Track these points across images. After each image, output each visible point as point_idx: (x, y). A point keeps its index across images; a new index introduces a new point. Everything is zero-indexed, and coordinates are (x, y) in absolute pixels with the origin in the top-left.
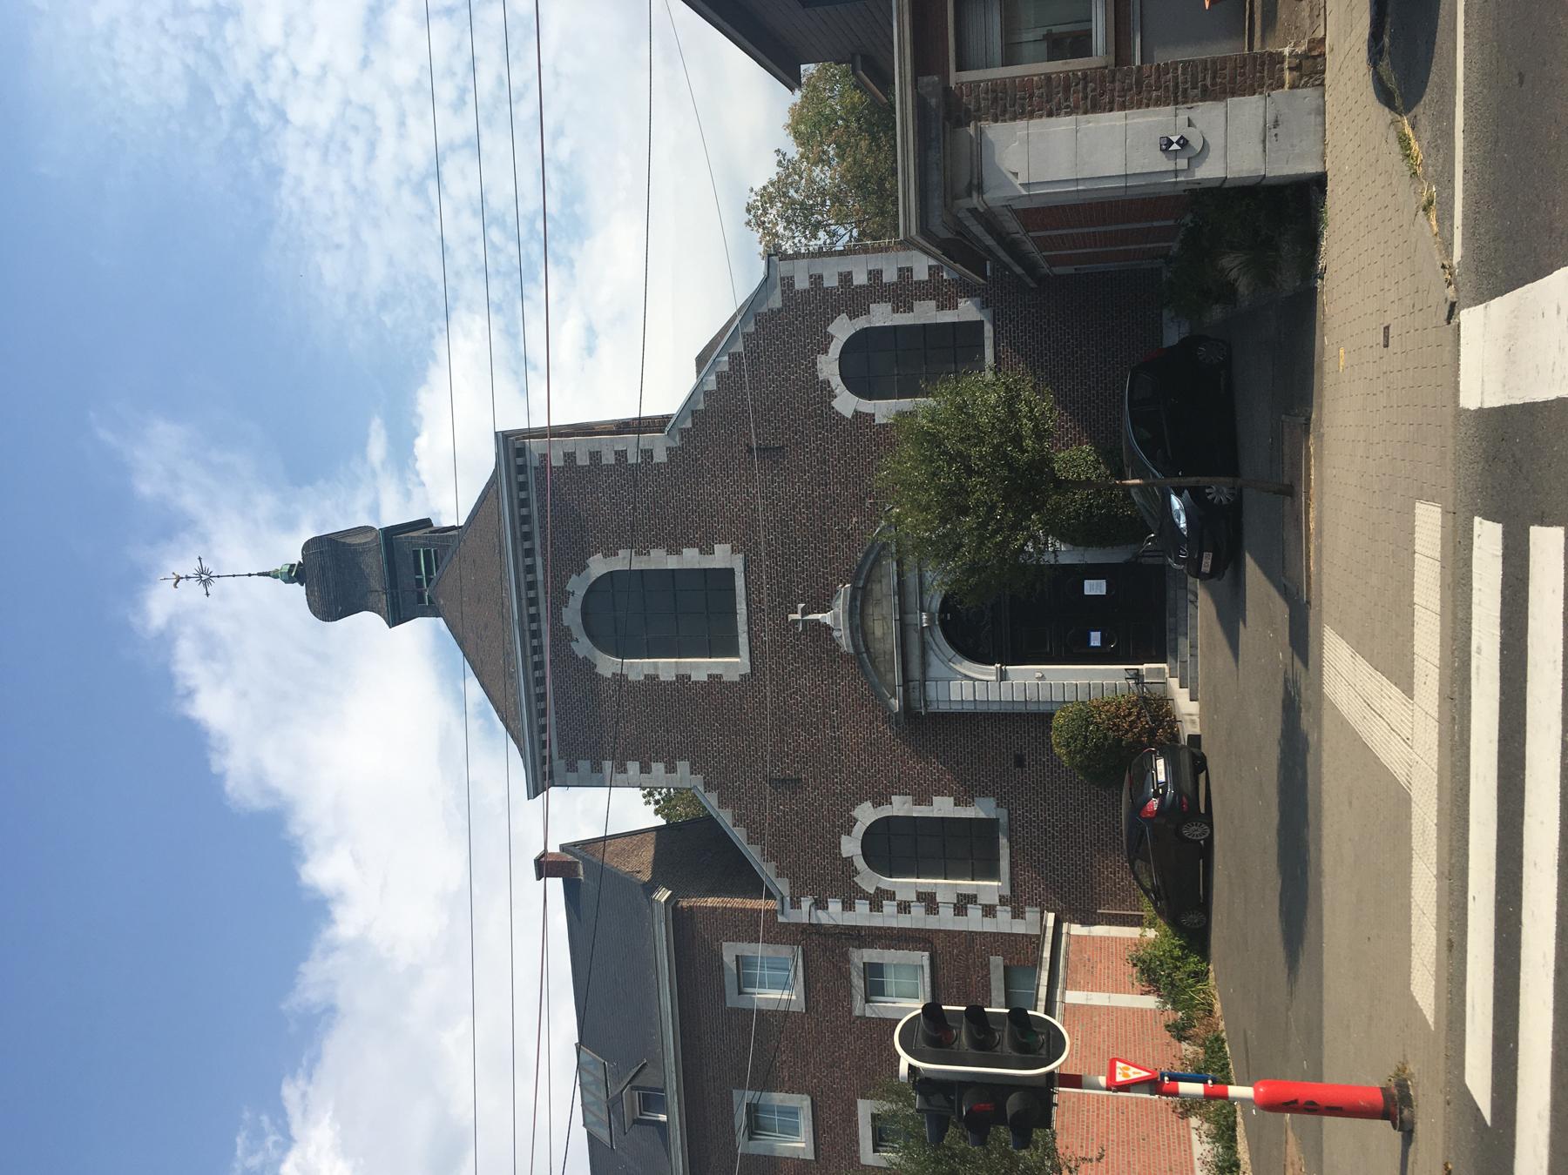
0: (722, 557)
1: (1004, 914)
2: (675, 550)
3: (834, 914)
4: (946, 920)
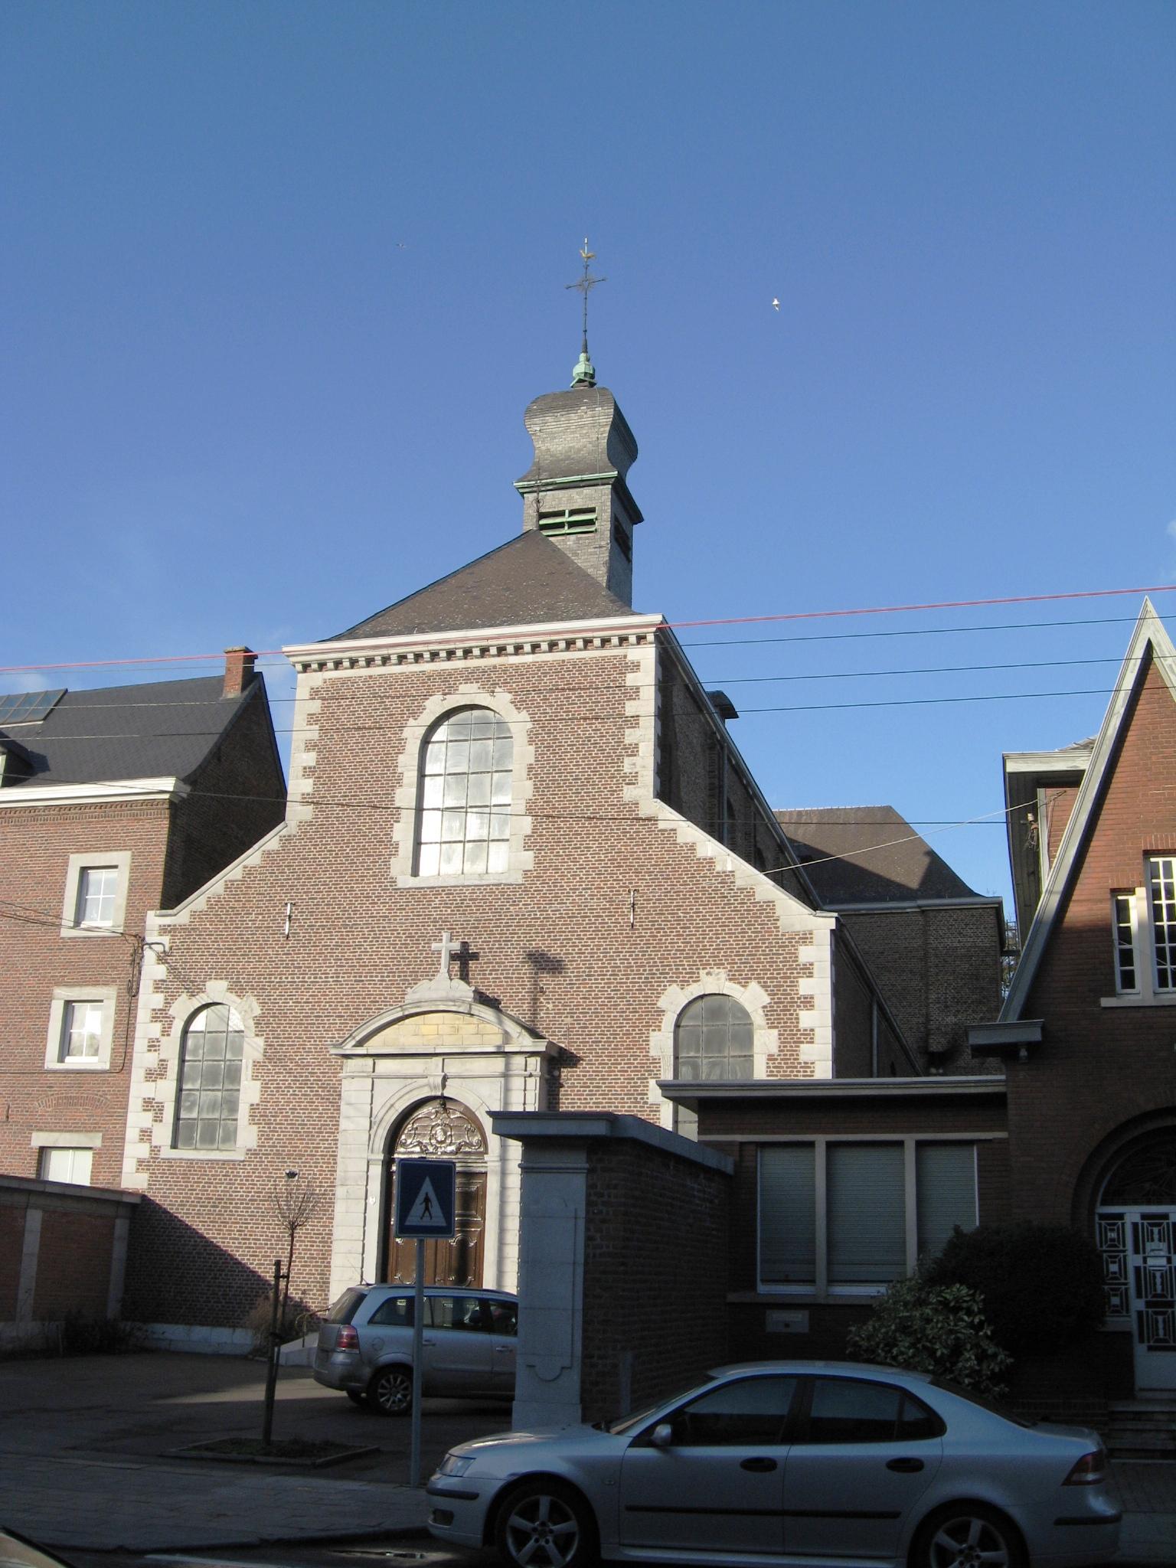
1: (143, 1151)
3: (153, 970)
4: (139, 1089)
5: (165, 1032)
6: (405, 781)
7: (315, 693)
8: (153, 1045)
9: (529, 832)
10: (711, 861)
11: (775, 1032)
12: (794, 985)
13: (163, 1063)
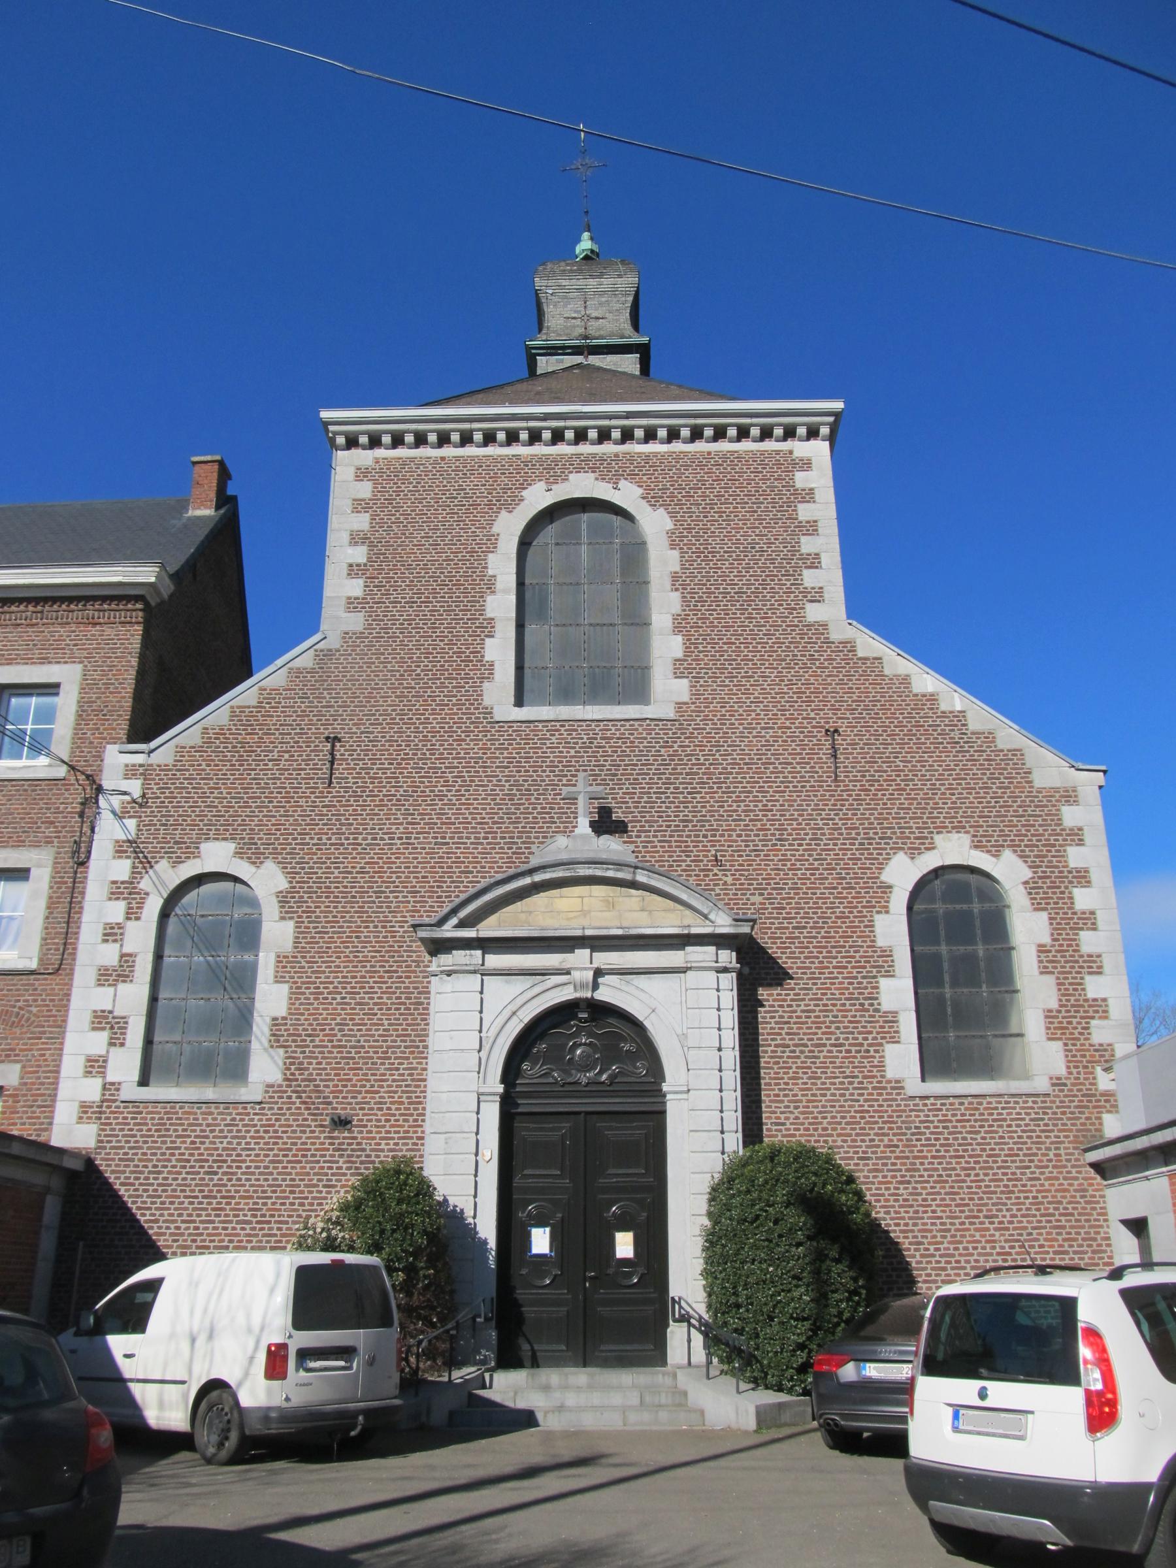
0: (668, 691)
1: (92, 1090)
2: (679, 625)
3: (110, 830)
4: (87, 995)
5: (132, 914)
6: (499, 585)
7: (362, 474)
8: (112, 933)
9: (680, 655)
10: (932, 698)
11: (1044, 915)
12: (1061, 856)
13: (127, 960)
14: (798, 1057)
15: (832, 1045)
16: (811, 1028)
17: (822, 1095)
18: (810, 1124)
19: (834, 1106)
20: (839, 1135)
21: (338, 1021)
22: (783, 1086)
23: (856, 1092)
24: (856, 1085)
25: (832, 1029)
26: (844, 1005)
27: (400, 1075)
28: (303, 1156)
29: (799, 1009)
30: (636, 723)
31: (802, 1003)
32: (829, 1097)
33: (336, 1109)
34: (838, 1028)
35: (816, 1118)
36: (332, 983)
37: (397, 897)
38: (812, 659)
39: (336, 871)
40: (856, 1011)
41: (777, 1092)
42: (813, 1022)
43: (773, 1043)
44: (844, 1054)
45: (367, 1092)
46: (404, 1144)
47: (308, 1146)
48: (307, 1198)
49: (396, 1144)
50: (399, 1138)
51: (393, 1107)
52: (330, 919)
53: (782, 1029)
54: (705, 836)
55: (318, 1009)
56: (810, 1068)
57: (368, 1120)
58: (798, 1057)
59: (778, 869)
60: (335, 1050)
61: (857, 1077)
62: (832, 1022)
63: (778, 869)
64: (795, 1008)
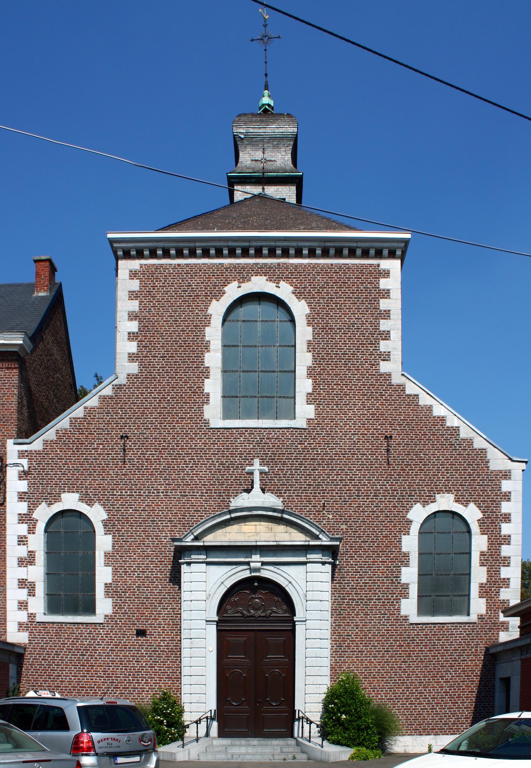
0: (305, 412)
1: (23, 616)
2: (311, 373)
5: (31, 531)
6: (212, 347)
7: (133, 275)
8: (22, 541)
9: (310, 391)
10: (443, 419)
11: (486, 537)
12: (498, 506)
13: (32, 554)
14: (359, 605)
15: (376, 599)
16: (366, 591)
17: (369, 623)
18: (363, 636)
19: (375, 628)
20: (376, 641)
21: (137, 585)
22: (351, 618)
23: (386, 621)
24: (386, 618)
25: (377, 592)
26: (384, 580)
27: (168, 611)
28: (125, 648)
29: (361, 582)
30: (285, 430)
31: (363, 579)
32: (373, 624)
33: (139, 627)
34: (379, 591)
35: (366, 633)
36: (133, 567)
37: (162, 524)
38: (381, 395)
39: (131, 510)
40: (389, 583)
41: (348, 621)
42: (368, 589)
43: (348, 598)
44: (381, 604)
45: (153, 619)
46: (171, 643)
47: (127, 644)
48: (128, 667)
49: (168, 643)
50: (169, 640)
51: (166, 626)
52: (129, 534)
53: (353, 591)
54: (319, 493)
55: (126, 579)
56: (365, 610)
57: (154, 632)
58: (359, 605)
59: (356, 511)
60: (136, 599)
61: (387, 614)
62: (377, 588)
63: (356, 511)
64: (359, 581)
